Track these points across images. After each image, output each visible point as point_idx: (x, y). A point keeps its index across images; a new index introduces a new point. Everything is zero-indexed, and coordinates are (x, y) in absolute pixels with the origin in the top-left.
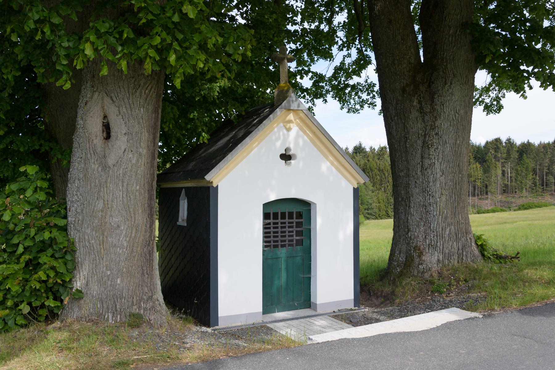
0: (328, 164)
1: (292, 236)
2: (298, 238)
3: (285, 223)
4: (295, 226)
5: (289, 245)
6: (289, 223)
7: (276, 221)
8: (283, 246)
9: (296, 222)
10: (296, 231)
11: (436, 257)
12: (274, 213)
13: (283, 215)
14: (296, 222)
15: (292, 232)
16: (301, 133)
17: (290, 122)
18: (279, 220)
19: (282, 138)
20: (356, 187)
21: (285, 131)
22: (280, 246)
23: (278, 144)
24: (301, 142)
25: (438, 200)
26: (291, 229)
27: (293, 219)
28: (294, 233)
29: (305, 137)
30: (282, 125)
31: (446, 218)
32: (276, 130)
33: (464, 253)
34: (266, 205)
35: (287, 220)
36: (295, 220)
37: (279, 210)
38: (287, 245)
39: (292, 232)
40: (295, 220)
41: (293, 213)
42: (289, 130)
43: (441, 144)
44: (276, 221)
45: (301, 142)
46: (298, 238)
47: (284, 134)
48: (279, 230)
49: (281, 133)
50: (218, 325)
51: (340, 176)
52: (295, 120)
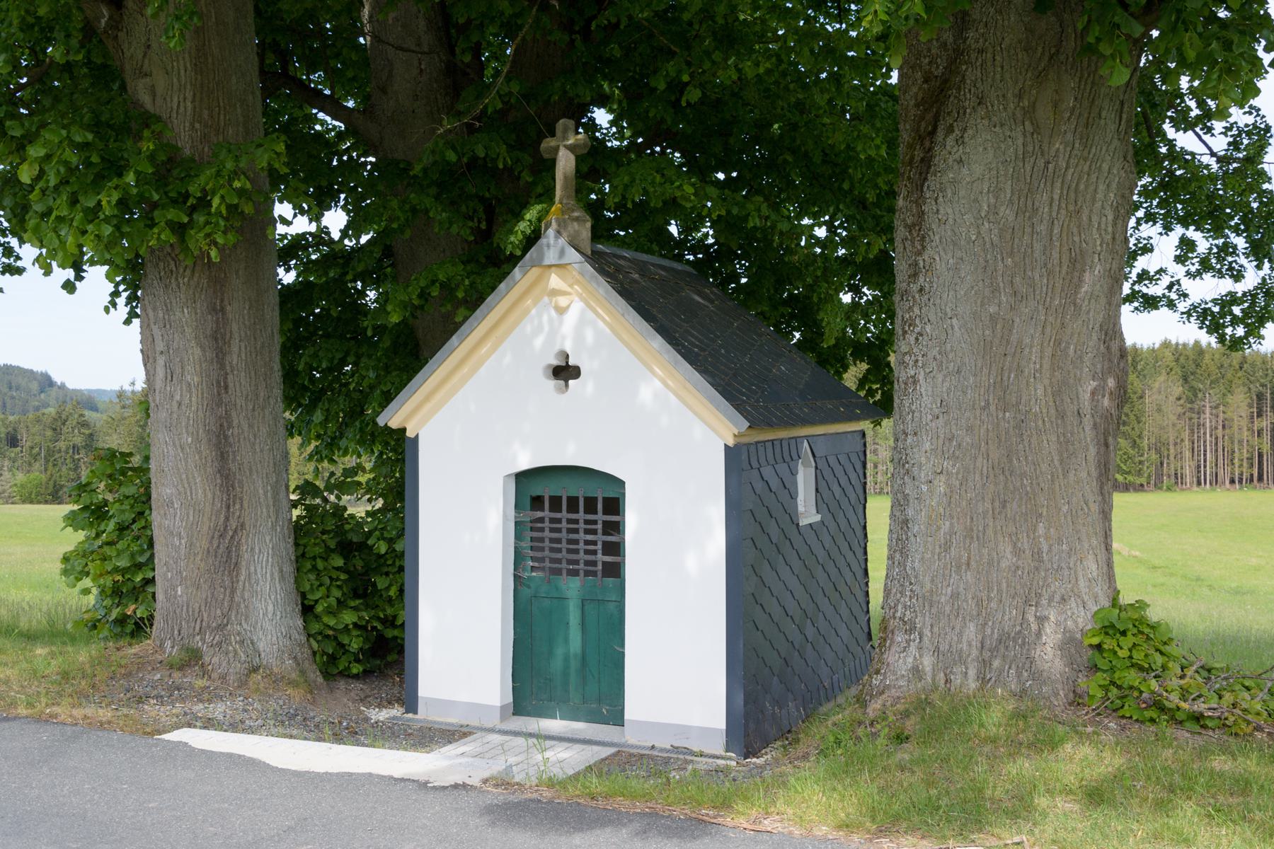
0: (658, 384)
1: (595, 553)
2: (608, 559)
3: (576, 521)
4: (600, 531)
5: (587, 574)
6: (587, 522)
7: (558, 515)
8: (574, 573)
9: (604, 523)
10: (604, 543)
11: (910, 660)
12: (551, 498)
13: (573, 504)
14: (604, 523)
15: (595, 543)
16: (591, 315)
17: (555, 293)
18: (564, 515)
19: (546, 328)
20: (731, 443)
21: (553, 313)
22: (564, 572)
23: (539, 342)
24: (589, 336)
25: (924, 488)
26: (590, 537)
27: (596, 513)
28: (599, 546)
29: (601, 324)
30: (546, 299)
31: (947, 547)
32: (533, 312)
33: (996, 663)
34: (523, 478)
35: (581, 515)
36: (600, 517)
37: (546, 489)
38: (582, 573)
39: (595, 543)
40: (600, 517)
41: (577, 498)
42: (561, 311)
43: (932, 317)
44: (539, 514)
45: (589, 336)
46: (608, 559)
47: (551, 320)
48: (564, 535)
49: (545, 318)
50: (416, 713)
51: (690, 414)
52: (571, 286)
